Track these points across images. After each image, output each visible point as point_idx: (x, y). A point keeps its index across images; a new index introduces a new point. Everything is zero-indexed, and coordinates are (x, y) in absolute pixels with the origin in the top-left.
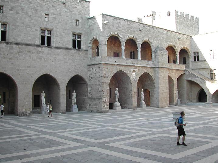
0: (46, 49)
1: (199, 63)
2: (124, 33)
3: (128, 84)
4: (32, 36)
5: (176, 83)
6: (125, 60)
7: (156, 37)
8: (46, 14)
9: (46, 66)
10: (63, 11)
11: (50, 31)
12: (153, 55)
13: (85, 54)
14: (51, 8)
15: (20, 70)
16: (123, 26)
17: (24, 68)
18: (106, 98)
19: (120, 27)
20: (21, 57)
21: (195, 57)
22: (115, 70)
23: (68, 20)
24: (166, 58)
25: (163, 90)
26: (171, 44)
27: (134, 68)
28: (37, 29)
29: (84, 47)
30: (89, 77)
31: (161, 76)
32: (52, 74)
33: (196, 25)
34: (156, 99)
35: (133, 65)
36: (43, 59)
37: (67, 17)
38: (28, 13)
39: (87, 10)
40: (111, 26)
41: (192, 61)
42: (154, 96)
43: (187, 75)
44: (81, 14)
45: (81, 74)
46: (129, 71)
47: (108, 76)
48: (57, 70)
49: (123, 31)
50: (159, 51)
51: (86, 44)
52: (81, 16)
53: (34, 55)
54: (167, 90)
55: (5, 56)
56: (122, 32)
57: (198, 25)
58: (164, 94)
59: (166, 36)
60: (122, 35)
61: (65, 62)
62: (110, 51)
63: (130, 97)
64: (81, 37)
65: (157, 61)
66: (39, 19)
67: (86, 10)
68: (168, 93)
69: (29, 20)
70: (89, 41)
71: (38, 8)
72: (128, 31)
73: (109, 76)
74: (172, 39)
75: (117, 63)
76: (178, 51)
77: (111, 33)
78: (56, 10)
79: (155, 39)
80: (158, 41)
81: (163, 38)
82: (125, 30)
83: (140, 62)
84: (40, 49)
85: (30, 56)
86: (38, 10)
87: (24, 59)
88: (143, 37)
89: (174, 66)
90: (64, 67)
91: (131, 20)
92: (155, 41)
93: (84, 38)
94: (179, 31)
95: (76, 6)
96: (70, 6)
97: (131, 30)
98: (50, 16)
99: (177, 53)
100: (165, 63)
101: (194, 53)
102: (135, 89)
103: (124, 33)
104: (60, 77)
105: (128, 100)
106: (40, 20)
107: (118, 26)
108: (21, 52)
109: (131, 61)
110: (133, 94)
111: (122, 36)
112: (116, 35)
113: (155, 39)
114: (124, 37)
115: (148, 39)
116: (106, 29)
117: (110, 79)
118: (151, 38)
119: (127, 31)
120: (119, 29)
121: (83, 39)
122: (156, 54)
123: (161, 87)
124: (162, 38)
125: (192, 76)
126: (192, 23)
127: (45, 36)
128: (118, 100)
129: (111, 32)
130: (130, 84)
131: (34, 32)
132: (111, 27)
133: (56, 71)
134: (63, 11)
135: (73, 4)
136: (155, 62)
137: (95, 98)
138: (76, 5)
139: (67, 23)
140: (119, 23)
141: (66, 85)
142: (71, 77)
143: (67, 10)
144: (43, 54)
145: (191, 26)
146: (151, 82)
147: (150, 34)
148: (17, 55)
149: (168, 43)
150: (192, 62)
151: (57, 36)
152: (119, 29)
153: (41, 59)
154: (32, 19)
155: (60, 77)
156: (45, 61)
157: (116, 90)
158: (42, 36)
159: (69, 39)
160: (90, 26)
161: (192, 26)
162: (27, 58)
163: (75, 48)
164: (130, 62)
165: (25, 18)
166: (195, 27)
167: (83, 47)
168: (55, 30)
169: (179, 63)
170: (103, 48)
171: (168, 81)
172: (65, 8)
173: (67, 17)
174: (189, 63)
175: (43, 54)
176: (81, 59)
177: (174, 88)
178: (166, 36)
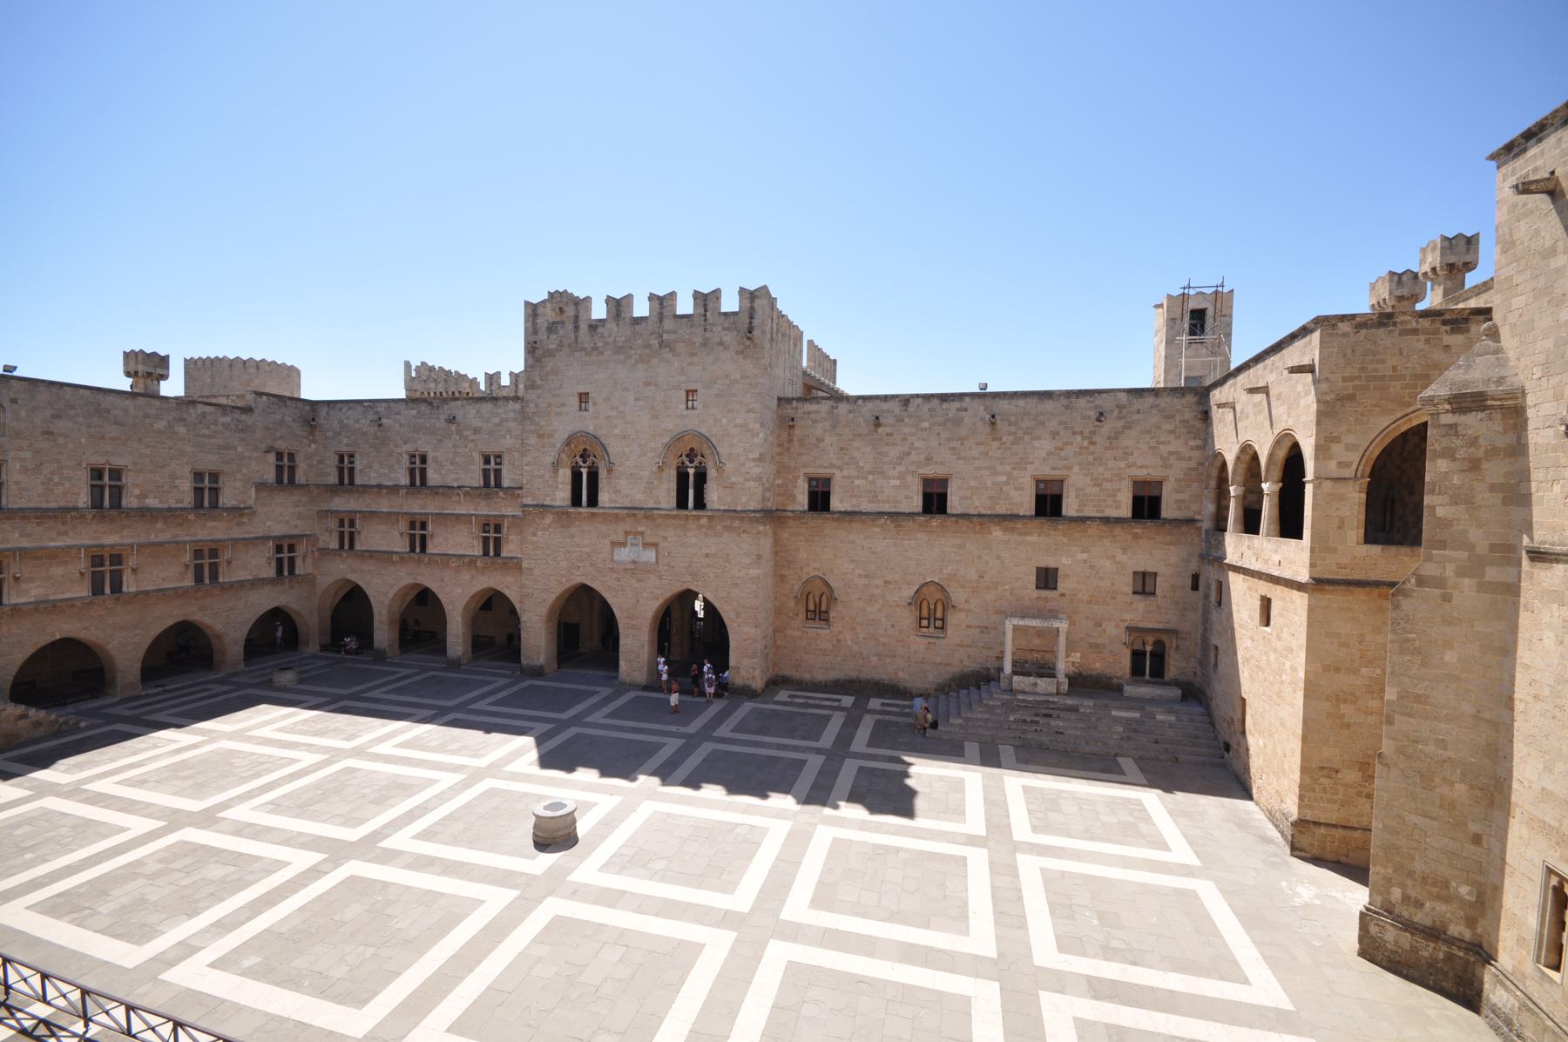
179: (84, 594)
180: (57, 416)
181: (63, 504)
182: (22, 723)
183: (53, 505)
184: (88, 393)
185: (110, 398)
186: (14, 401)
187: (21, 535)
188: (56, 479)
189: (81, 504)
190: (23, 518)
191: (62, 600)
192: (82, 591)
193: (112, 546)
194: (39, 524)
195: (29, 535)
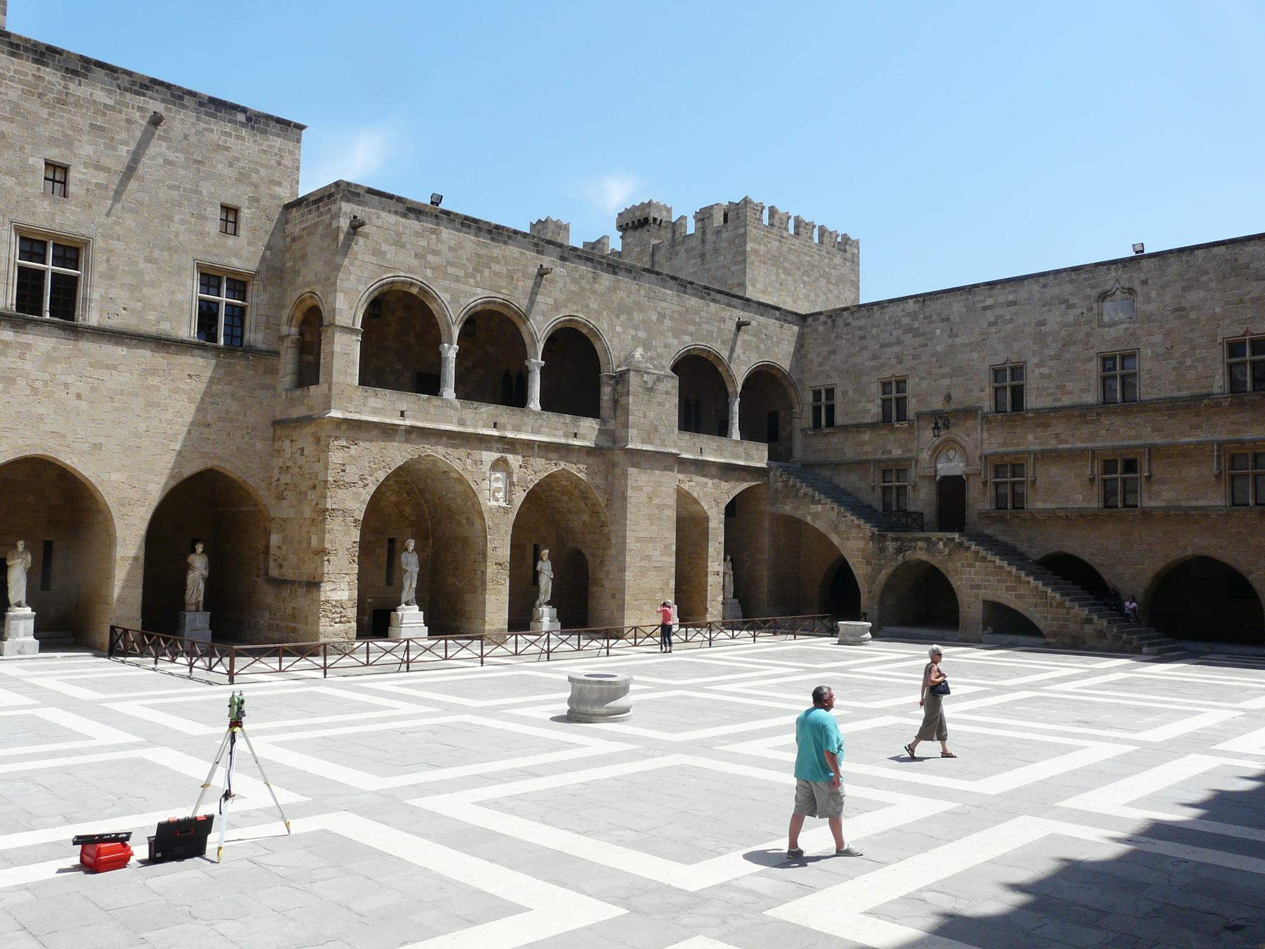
0: (43, 343)
1: (835, 440)
2: (457, 279)
3: (470, 522)
5: (722, 526)
6: (456, 409)
7: (622, 310)
8: (49, 165)
9: (41, 418)
10: (153, 158)
11: (70, 252)
12: (606, 391)
13: (261, 369)
14: (85, 138)
16: (450, 249)
18: (341, 589)
19: (436, 253)
21: (817, 410)
22: (398, 454)
23: (180, 205)
24: (667, 405)
25: (649, 558)
26: (702, 344)
27: (500, 446)
29: (260, 336)
30: (278, 480)
31: (639, 489)
32: (69, 459)
33: (845, 270)
34: (613, 596)
35: (495, 433)
36: (21, 382)
37: (171, 187)
39: (284, 162)
40: (386, 241)
41: (806, 426)
42: (605, 583)
43: (776, 491)
44: (254, 178)
45: (234, 467)
46: (475, 462)
47: (356, 479)
48: (101, 440)
49: (451, 270)
50: (633, 379)
51: (271, 325)
52: (249, 189)
54: (664, 558)
57: (856, 273)
58: (652, 574)
59: (677, 308)
60: (446, 290)
61: (150, 404)
62: (399, 366)
63: (478, 585)
64: (250, 288)
65: (620, 419)
67: (279, 163)
68: (673, 570)
70: (286, 313)
74: (709, 322)
75: (408, 422)
76: (733, 382)
77: (388, 276)
78: (115, 148)
79: (618, 316)
80: (636, 328)
81: (662, 316)
82: (463, 267)
83: (536, 424)
88: (556, 307)
89: (712, 450)
90: (142, 427)
91: (495, 220)
92: (618, 329)
93: (264, 297)
94: (764, 292)
95: (225, 141)
96: (193, 139)
97: (497, 268)
98: (78, 176)
99: (730, 390)
100: (662, 429)
101: (817, 394)
102: (499, 547)
103: (457, 279)
104: (115, 477)
105: (468, 597)
106: (18, 188)
107: (424, 243)
109: (485, 415)
110: (491, 570)
111: (445, 297)
112: (414, 291)
113: (618, 316)
114: (455, 300)
115: (581, 316)
116: (360, 257)
118: (599, 313)
120: (430, 258)
121: (256, 300)
122: (619, 387)
123: (638, 540)
124: (654, 318)
125: (796, 496)
126: (826, 261)
127: (41, 273)
128: (412, 595)
129: (388, 269)
130: (478, 525)
132: (384, 247)
133: (97, 447)
134: (153, 158)
135: (212, 131)
136: (611, 425)
137: (292, 583)
138: (229, 135)
139: (170, 219)
140: (433, 232)
141: (149, 516)
142: (180, 479)
143: (172, 156)
144: (22, 357)
145: (821, 276)
146: (591, 517)
147: (594, 292)
149: (687, 339)
150: (803, 430)
151: (113, 278)
155: (115, 477)
156: (35, 391)
158: (22, 270)
159: (179, 296)
160: (294, 240)
161: (827, 276)
163: (214, 338)
164: (482, 419)
166: (841, 280)
167: (254, 336)
168: (99, 243)
169: (736, 434)
170: (344, 353)
171: (671, 514)
172: (164, 144)
173: (171, 187)
174: (790, 438)
175: (22, 357)
176: (241, 392)
177: (711, 549)
178: (677, 308)
179: (1220, 502)
180: (1186, 289)
181: (1196, 391)
182: (1087, 628)
183: (1185, 393)
184: (1222, 249)
185: (1249, 249)
186: (1145, 282)
187: (1153, 431)
188: (1188, 362)
189: (1216, 390)
190: (1155, 410)
191: (1196, 508)
192: (1217, 499)
193: (1254, 442)
194: (1170, 417)
195: (1160, 430)
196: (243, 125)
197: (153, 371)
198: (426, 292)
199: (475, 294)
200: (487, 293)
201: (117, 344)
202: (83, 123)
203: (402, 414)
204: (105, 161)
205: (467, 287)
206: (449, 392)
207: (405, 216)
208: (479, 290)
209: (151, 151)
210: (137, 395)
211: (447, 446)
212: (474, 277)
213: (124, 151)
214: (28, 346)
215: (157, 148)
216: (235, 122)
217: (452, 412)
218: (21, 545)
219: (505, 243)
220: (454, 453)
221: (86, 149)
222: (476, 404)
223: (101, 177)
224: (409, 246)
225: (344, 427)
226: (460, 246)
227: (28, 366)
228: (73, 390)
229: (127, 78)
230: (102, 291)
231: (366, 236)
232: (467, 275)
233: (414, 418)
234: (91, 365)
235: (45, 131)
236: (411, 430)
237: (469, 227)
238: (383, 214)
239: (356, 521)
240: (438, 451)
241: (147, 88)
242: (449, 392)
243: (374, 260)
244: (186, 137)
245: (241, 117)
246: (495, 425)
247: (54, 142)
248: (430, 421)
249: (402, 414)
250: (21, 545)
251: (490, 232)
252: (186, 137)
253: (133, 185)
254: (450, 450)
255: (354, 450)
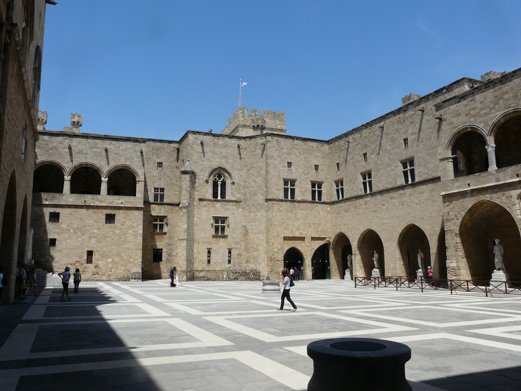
2: (486, 114)
4: (393, 177)
15: (384, 223)
16: (481, 103)
17: (387, 221)
20: (384, 207)
22: (469, 203)
28: (397, 164)
36: (405, 204)
37: (429, 129)
38: (386, 149)
46: (507, 198)
47: (454, 217)
48: (423, 216)
49: (482, 112)
53: (396, 200)
55: (371, 210)
56: (480, 116)
60: (481, 122)
66: (397, 150)
69: (389, 158)
71: (395, 136)
72: (498, 104)
73: (456, 216)
77: (455, 130)
84: (401, 192)
85: (392, 203)
86: (395, 139)
87: (387, 209)
103: (486, 114)
104: (428, 227)
108: (384, 201)
109: (510, 173)
111: (481, 126)
112: (469, 130)
114: (486, 124)
117: (458, 222)
119: (492, 106)
120: (472, 112)
131: (393, 170)
132: (452, 120)
148: (381, 206)
152: (472, 112)
153: (403, 204)
154: (390, 154)
157: (495, 244)
162: (390, 207)
165: (384, 156)
196: (446, 93)
197: (432, 190)
198: (474, 128)
199: (496, 116)
200: (503, 112)
201: (423, 185)
202: (408, 123)
203: (469, 185)
204: (414, 131)
205: (492, 115)
206: (493, 167)
207: (459, 102)
208: (498, 113)
209: (424, 120)
210: (429, 199)
211: (491, 194)
212: (494, 108)
213: (418, 125)
214: (405, 193)
215: (426, 117)
216: (443, 94)
217: (492, 176)
218: (420, 251)
219: (510, 81)
220: (495, 196)
221: (410, 131)
222: (504, 169)
223: (414, 136)
224: (462, 113)
225: (447, 197)
226: (486, 98)
227: (406, 199)
228: (415, 203)
229: (416, 103)
230: (418, 170)
231: (445, 120)
232: (491, 109)
233: (475, 185)
234: (419, 194)
235: (402, 132)
236: (473, 191)
237: (489, 86)
238: (450, 107)
239: (456, 234)
240: (487, 197)
241: (420, 102)
242: (493, 167)
243: (450, 127)
244: (431, 109)
245: (445, 91)
246: (518, 176)
247: (404, 133)
248: (481, 184)
249: (469, 185)
250: (420, 251)
251: (501, 81)
252: (431, 109)
253: (421, 133)
254: (492, 195)
255: (451, 206)
